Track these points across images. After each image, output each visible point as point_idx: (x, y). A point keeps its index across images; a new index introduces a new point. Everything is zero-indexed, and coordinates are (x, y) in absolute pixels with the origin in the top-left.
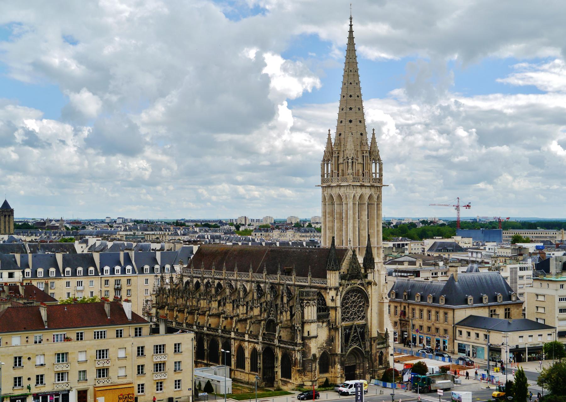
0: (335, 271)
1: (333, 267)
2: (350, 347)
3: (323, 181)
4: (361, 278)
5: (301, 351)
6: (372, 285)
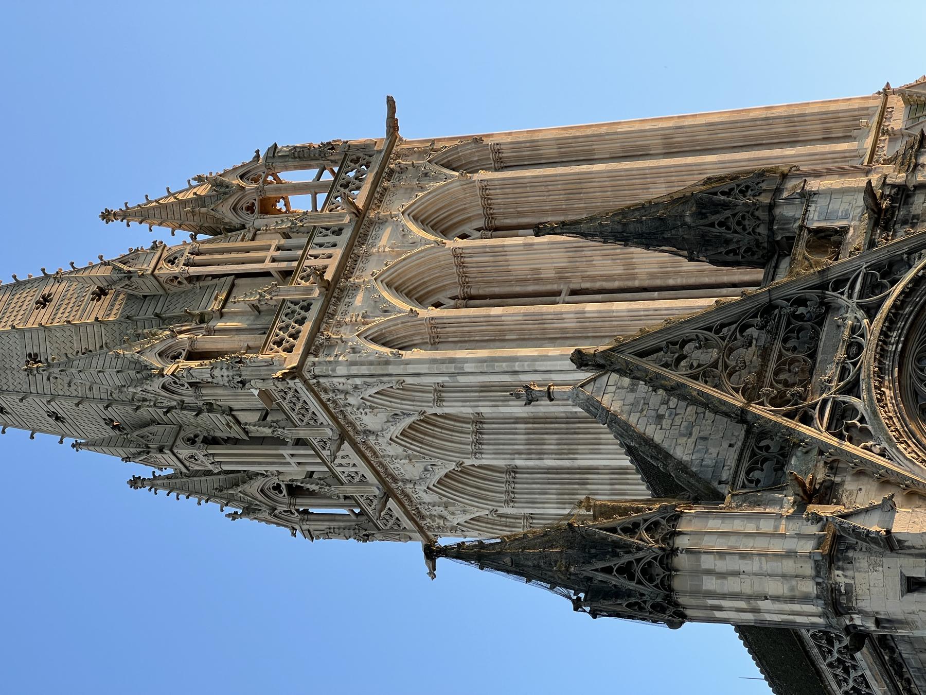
0: (674, 551)
1: (638, 574)
3: (396, 533)
4: (823, 286)
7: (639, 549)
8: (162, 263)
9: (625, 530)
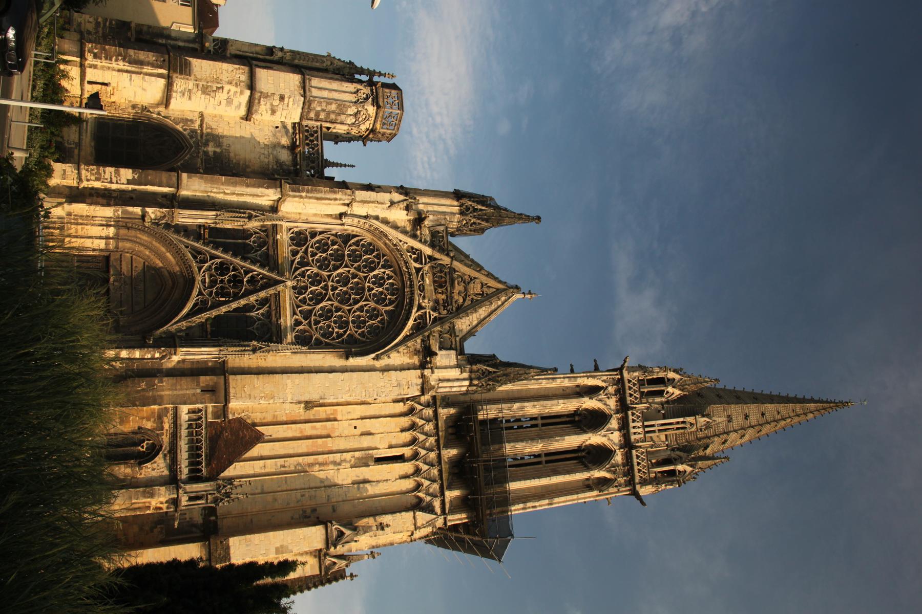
2: (196, 253)
5: (196, 46)
6: (419, 372)
7: (469, 201)
8: (694, 422)
9: (477, 209)
